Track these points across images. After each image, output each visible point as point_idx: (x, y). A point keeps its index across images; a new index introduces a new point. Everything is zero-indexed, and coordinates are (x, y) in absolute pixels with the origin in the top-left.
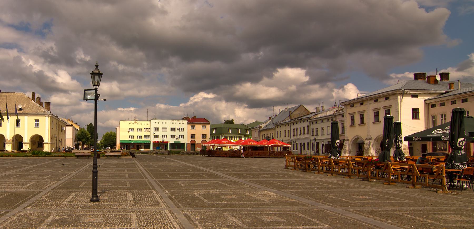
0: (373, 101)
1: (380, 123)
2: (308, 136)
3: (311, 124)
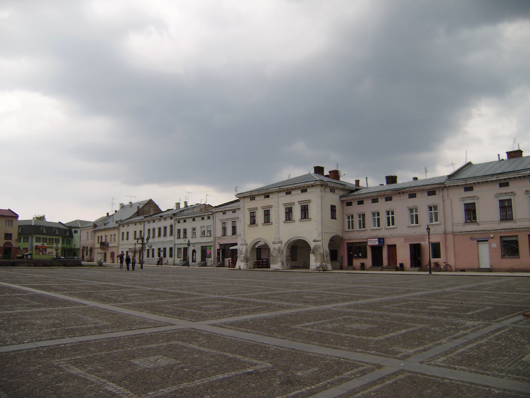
0: (285, 194)
1: (272, 224)
2: (172, 238)
3: (177, 222)
